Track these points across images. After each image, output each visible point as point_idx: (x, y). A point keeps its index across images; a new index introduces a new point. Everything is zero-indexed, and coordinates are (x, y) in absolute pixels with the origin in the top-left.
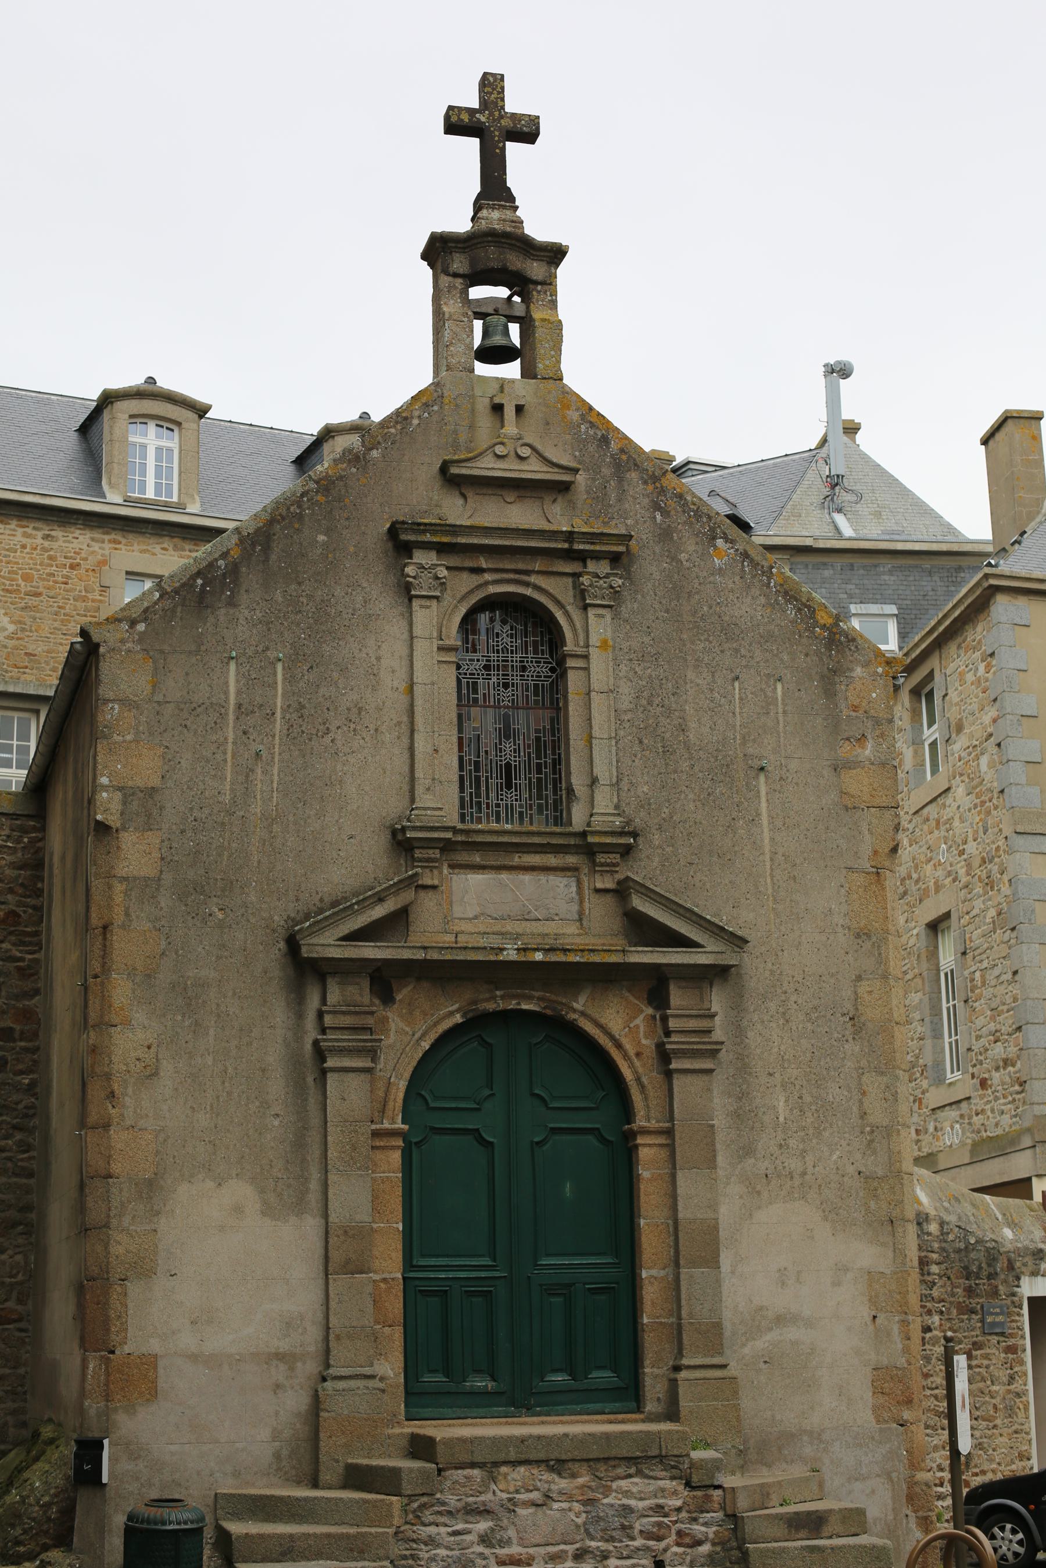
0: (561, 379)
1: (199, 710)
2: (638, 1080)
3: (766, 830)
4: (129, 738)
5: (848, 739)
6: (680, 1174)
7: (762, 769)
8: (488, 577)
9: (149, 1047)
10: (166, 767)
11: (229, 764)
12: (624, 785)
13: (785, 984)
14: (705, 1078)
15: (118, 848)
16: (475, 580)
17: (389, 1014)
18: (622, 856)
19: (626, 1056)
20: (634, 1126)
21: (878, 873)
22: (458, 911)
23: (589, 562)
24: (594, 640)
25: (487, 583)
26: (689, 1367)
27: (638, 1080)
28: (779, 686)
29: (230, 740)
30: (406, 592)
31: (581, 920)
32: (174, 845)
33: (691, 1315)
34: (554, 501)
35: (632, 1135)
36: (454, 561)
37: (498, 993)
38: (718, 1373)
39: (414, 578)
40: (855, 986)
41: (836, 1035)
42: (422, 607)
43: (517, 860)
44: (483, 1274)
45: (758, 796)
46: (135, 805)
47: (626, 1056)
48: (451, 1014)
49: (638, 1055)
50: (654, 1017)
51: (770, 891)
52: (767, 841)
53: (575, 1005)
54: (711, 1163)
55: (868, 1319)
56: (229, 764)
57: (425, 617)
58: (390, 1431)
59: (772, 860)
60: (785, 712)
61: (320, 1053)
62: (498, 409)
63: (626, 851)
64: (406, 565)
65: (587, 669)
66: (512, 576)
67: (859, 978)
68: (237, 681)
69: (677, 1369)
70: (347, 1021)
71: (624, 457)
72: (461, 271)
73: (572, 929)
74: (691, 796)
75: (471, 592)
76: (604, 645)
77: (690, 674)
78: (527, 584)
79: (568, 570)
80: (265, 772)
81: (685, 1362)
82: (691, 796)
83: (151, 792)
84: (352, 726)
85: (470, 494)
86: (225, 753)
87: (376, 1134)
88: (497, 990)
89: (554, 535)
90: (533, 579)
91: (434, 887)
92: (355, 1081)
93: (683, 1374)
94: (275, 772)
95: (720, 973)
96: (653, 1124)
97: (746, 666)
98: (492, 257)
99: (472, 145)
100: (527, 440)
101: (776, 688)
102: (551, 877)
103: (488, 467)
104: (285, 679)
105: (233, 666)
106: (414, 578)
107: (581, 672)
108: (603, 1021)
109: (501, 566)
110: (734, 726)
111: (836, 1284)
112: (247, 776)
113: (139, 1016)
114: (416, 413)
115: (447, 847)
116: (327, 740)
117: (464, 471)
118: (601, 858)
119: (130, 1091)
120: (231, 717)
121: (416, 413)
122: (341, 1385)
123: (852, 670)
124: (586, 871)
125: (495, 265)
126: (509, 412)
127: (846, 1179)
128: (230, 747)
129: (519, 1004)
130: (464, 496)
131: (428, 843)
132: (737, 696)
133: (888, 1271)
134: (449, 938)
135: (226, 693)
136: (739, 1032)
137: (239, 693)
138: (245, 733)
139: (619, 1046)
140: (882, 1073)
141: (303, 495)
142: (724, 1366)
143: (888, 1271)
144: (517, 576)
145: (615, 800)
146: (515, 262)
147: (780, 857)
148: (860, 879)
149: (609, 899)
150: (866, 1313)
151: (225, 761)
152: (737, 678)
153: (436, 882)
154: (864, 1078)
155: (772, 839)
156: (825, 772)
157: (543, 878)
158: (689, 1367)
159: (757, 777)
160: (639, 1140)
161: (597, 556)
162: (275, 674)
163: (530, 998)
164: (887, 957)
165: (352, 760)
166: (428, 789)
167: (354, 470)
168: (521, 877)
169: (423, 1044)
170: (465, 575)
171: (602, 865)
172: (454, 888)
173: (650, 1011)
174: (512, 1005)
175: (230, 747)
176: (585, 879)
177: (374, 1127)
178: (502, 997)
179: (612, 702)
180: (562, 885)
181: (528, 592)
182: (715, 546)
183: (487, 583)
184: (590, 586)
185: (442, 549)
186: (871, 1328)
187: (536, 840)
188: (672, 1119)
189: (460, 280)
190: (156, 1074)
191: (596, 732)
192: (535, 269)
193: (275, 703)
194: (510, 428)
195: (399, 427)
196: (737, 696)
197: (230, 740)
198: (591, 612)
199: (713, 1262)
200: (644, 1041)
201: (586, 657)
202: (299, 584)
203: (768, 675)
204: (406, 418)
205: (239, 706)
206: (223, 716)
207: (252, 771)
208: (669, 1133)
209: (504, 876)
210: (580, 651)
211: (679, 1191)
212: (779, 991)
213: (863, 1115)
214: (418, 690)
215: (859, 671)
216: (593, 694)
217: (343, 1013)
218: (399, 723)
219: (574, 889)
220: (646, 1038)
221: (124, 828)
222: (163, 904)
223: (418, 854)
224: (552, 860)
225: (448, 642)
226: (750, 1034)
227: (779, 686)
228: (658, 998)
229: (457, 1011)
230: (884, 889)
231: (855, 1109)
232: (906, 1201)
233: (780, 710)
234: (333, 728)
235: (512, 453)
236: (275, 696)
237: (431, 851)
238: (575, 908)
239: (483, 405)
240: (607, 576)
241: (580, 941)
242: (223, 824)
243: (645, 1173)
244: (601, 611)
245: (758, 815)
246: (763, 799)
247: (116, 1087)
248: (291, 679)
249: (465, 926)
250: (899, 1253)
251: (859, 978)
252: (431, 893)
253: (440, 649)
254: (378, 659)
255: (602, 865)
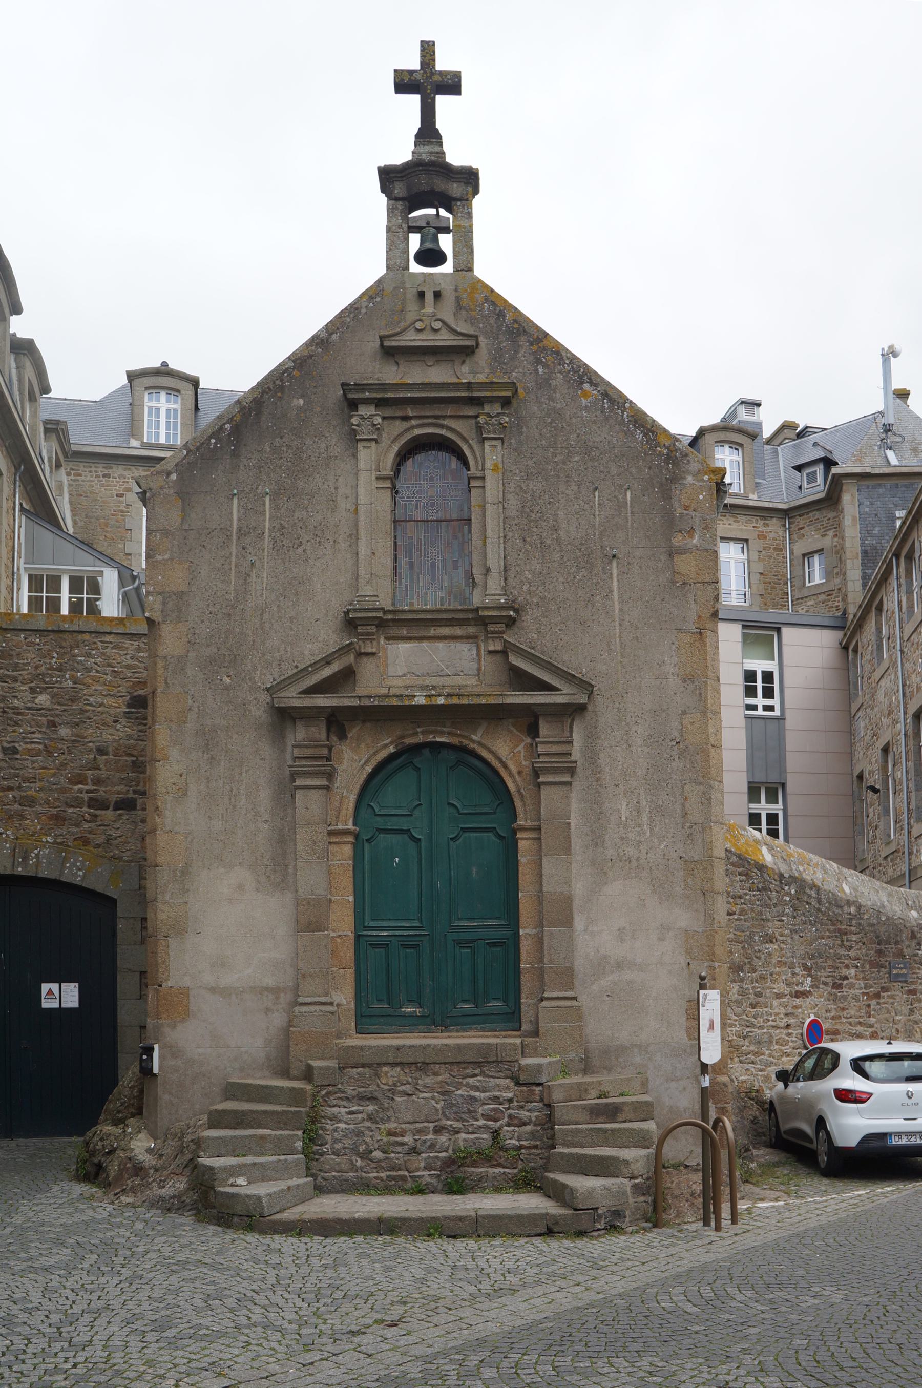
0: (470, 269)
1: (213, 534)
2: (519, 791)
3: (616, 603)
4: (167, 557)
5: (680, 532)
6: (545, 861)
7: (614, 556)
8: (414, 422)
9: (181, 775)
10: (191, 577)
11: (233, 572)
12: (511, 574)
13: (628, 718)
14: (565, 788)
15: (160, 635)
16: (406, 425)
17: (344, 747)
18: (506, 626)
19: (511, 775)
20: (515, 825)
21: (700, 633)
22: (391, 671)
23: (485, 406)
24: (489, 465)
25: (413, 427)
26: (548, 999)
27: (519, 791)
28: (629, 493)
29: (234, 554)
30: (353, 438)
31: (478, 675)
32: (197, 632)
33: (551, 962)
34: (463, 362)
35: (514, 832)
36: (388, 412)
37: (419, 730)
38: (568, 1003)
39: (357, 425)
40: (681, 718)
41: (666, 755)
42: (364, 447)
43: (432, 632)
44: (406, 933)
45: (611, 578)
46: (170, 605)
47: (511, 775)
48: (386, 746)
49: (519, 773)
50: (532, 745)
51: (618, 648)
52: (617, 611)
53: (474, 737)
54: (568, 850)
55: (684, 965)
56: (233, 572)
57: (366, 455)
58: (337, 1041)
59: (620, 625)
60: (632, 513)
61: (293, 776)
62: (421, 295)
63: (511, 622)
64: (352, 416)
65: (484, 487)
66: (430, 421)
67: (684, 713)
68: (238, 511)
69: (542, 1000)
70: (308, 752)
71: (516, 326)
72: (400, 195)
73: (473, 681)
74: (561, 579)
75: (401, 434)
76: (495, 469)
77: (562, 488)
78: (442, 426)
79: (471, 414)
80: (258, 576)
81: (546, 995)
82: (561, 579)
83: (180, 595)
84: (318, 539)
85: (401, 362)
86: (230, 564)
87: (331, 833)
88: (419, 727)
89: (457, 386)
90: (446, 422)
91: (373, 654)
92: (315, 795)
93: (544, 1003)
94: (265, 576)
95: (579, 709)
96: (529, 823)
97: (603, 479)
98: (423, 182)
99: (414, 101)
100: (439, 317)
101: (626, 495)
102: (459, 644)
103: (411, 339)
104: (270, 508)
105: (235, 501)
106: (357, 425)
107: (481, 490)
108: (494, 749)
109: (423, 414)
110: (594, 525)
111: (661, 939)
112: (245, 580)
113: (174, 753)
114: (364, 305)
115: (381, 624)
116: (300, 550)
117: (394, 344)
118: (491, 628)
119: (169, 806)
120: (234, 538)
121: (364, 305)
122: (304, 1009)
123: (685, 478)
124: (483, 638)
125: (426, 188)
126: (429, 297)
127: (670, 862)
128: (234, 559)
129: (434, 737)
130: (397, 363)
131: (367, 621)
132: (597, 503)
133: (700, 930)
134: (384, 691)
135: (231, 520)
136: (591, 755)
137: (239, 519)
138: (244, 549)
139: (506, 767)
140: (701, 784)
141: (283, 373)
142: (575, 998)
143: (700, 930)
144: (434, 421)
145: (503, 584)
146: (440, 185)
147: (626, 623)
148: (687, 638)
149: (498, 658)
150: (683, 960)
151: (231, 569)
152: (596, 489)
153: (374, 650)
154: (686, 788)
155: (621, 610)
156: (662, 557)
157: (452, 644)
158: (548, 999)
159: (610, 562)
160: (518, 836)
161: (491, 400)
162: (264, 505)
163: (442, 733)
164: (706, 697)
165: (318, 564)
166: (368, 582)
167: (320, 350)
168: (437, 644)
169: (367, 768)
170: (398, 422)
171: (492, 633)
172: (389, 655)
173: (529, 740)
174: (430, 738)
175: (234, 559)
176: (482, 644)
177: (330, 828)
178: (423, 733)
179: (501, 511)
180: (466, 650)
181: (443, 432)
182: (582, 389)
183: (413, 427)
184: (486, 423)
185: (380, 403)
186: (686, 971)
187: (444, 616)
188: (539, 819)
189: (401, 203)
190: (185, 794)
191: (489, 533)
192: (455, 189)
193: (264, 526)
194: (429, 308)
195: (352, 316)
196: (597, 503)
197: (234, 554)
198: (487, 444)
199: (568, 922)
200: (524, 763)
201: (483, 478)
202: (281, 438)
203: (621, 486)
204: (357, 309)
205: (240, 529)
206: (229, 537)
207: (249, 575)
208: (538, 829)
209: (425, 644)
210: (479, 474)
211: (544, 872)
212: (624, 723)
213: (685, 815)
214: (361, 509)
215: (690, 479)
216: (488, 505)
217: (306, 746)
218: (351, 535)
219: (475, 652)
220: (526, 760)
221: (164, 622)
222: (189, 674)
223: (360, 629)
224: (458, 631)
225: (384, 473)
226: (602, 756)
227: (629, 493)
228: (533, 731)
229: (391, 743)
230: (705, 645)
231: (679, 811)
232: (716, 878)
233: (629, 512)
234: (304, 542)
235: (429, 327)
236: (264, 520)
237: (369, 627)
238: (476, 666)
239: (411, 294)
240: (498, 415)
241: (477, 690)
242: (229, 615)
243: (523, 860)
244: (494, 443)
245: (611, 591)
246: (615, 580)
247: (159, 804)
248: (276, 508)
249: (396, 682)
250: (709, 917)
251: (684, 713)
252: (371, 659)
253: (378, 478)
254: (336, 489)
255: (492, 633)
